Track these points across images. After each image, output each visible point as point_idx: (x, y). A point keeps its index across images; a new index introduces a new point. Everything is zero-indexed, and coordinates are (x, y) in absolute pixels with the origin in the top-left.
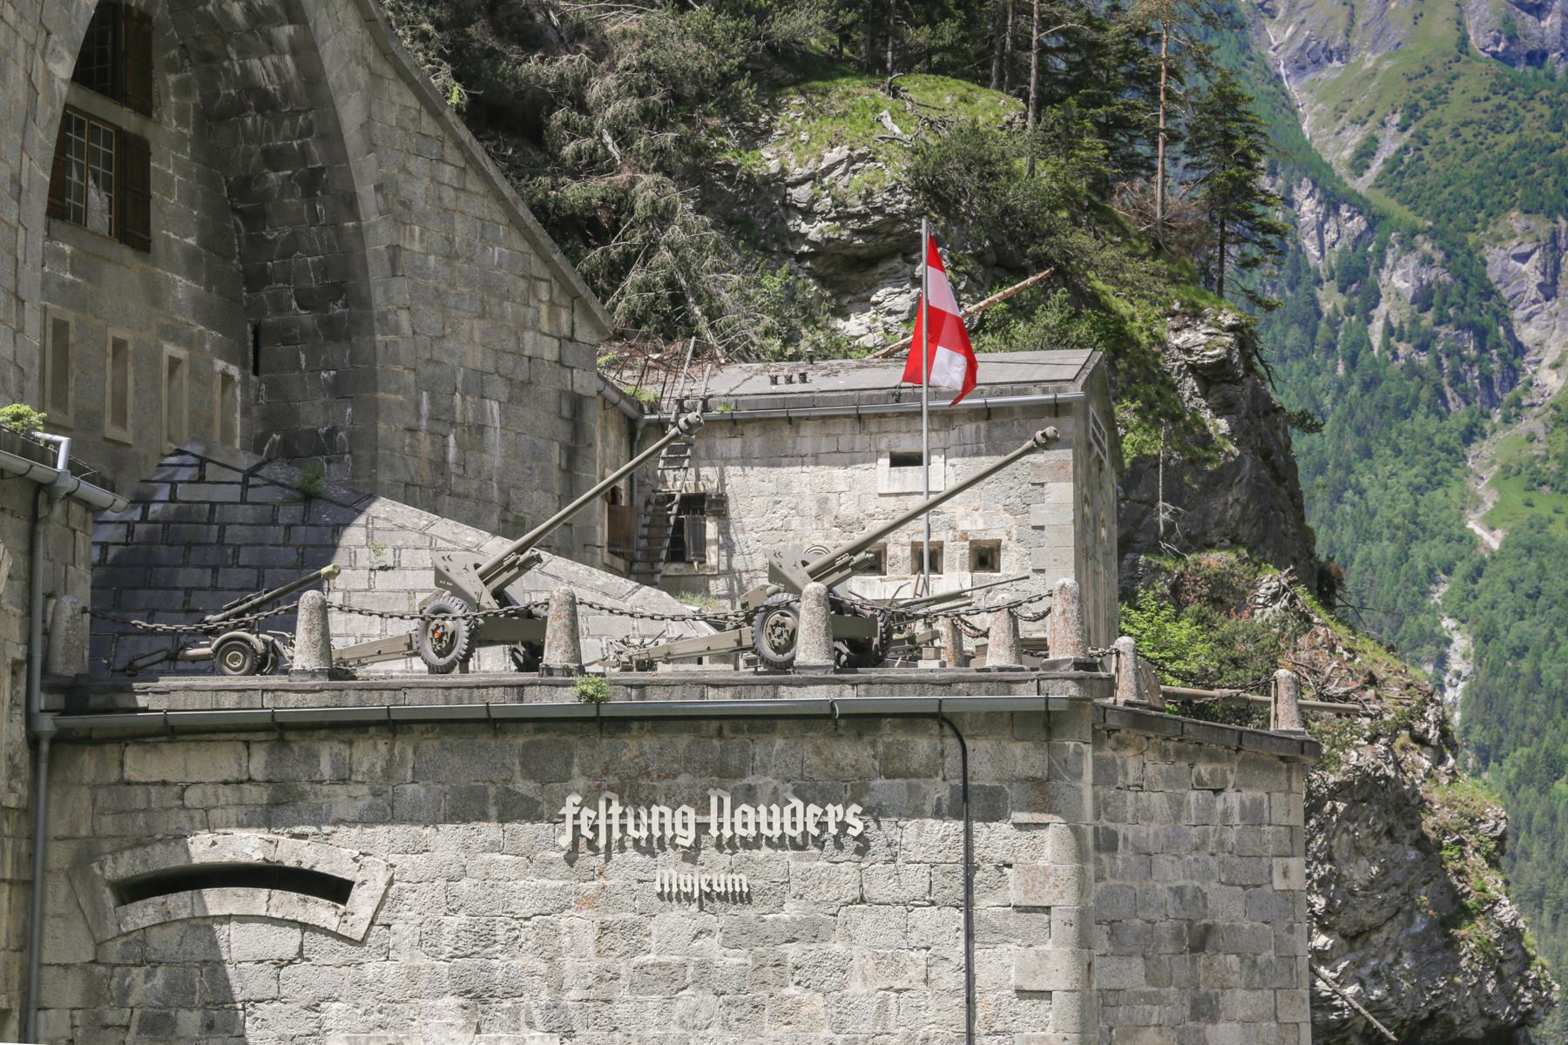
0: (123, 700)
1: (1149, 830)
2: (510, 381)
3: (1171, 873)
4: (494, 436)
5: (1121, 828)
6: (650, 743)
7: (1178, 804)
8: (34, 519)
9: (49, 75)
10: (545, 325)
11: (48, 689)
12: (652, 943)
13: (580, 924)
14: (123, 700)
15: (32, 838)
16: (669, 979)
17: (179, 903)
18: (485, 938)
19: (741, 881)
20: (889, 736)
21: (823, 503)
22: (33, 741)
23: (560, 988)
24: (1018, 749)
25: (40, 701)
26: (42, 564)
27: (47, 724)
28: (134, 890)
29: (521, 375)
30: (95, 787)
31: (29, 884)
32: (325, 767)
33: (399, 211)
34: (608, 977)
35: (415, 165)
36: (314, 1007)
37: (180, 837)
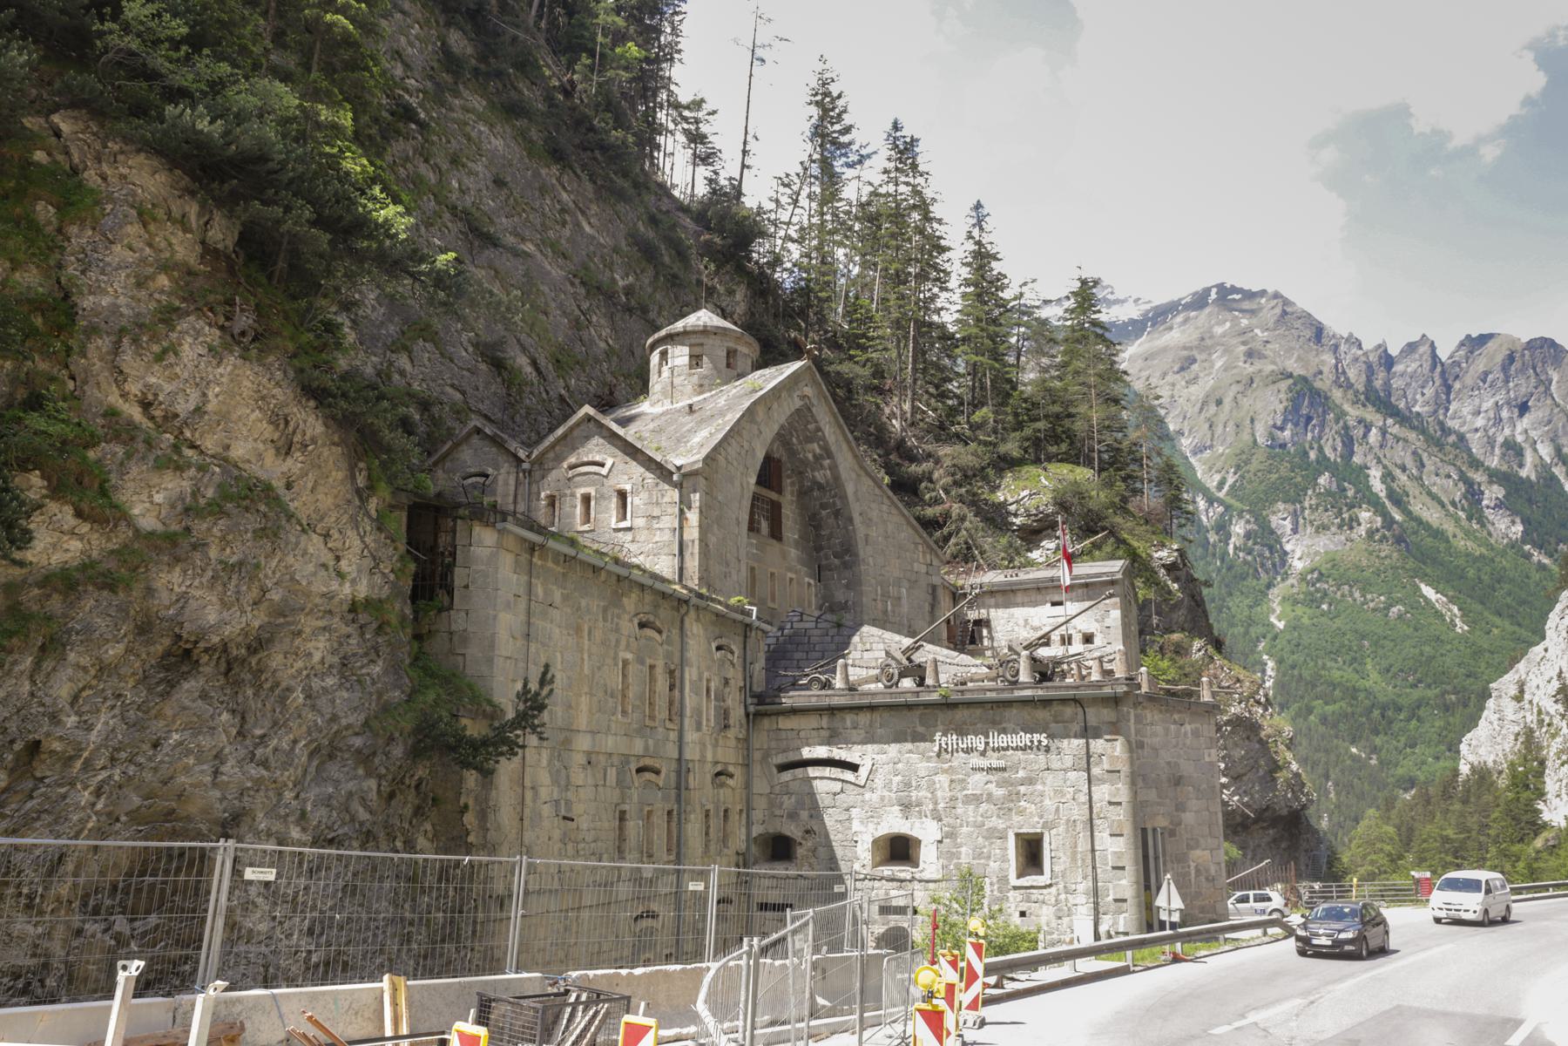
0: (777, 700)
1: (1156, 740)
4: (904, 601)
5: (1145, 740)
7: (1167, 730)
8: (746, 637)
9: (748, 483)
10: (921, 560)
11: (752, 697)
12: (970, 786)
13: (943, 780)
14: (777, 700)
15: (748, 749)
16: (976, 799)
17: (799, 772)
18: (908, 785)
19: (1002, 763)
20: (1056, 708)
21: (1026, 621)
22: (747, 715)
23: (936, 803)
24: (1105, 711)
25: (749, 701)
26: (748, 652)
27: (752, 709)
28: (784, 768)
29: (913, 579)
30: (768, 731)
31: (747, 765)
33: (868, 522)
34: (953, 799)
35: (873, 506)
36: (847, 810)
37: (799, 749)
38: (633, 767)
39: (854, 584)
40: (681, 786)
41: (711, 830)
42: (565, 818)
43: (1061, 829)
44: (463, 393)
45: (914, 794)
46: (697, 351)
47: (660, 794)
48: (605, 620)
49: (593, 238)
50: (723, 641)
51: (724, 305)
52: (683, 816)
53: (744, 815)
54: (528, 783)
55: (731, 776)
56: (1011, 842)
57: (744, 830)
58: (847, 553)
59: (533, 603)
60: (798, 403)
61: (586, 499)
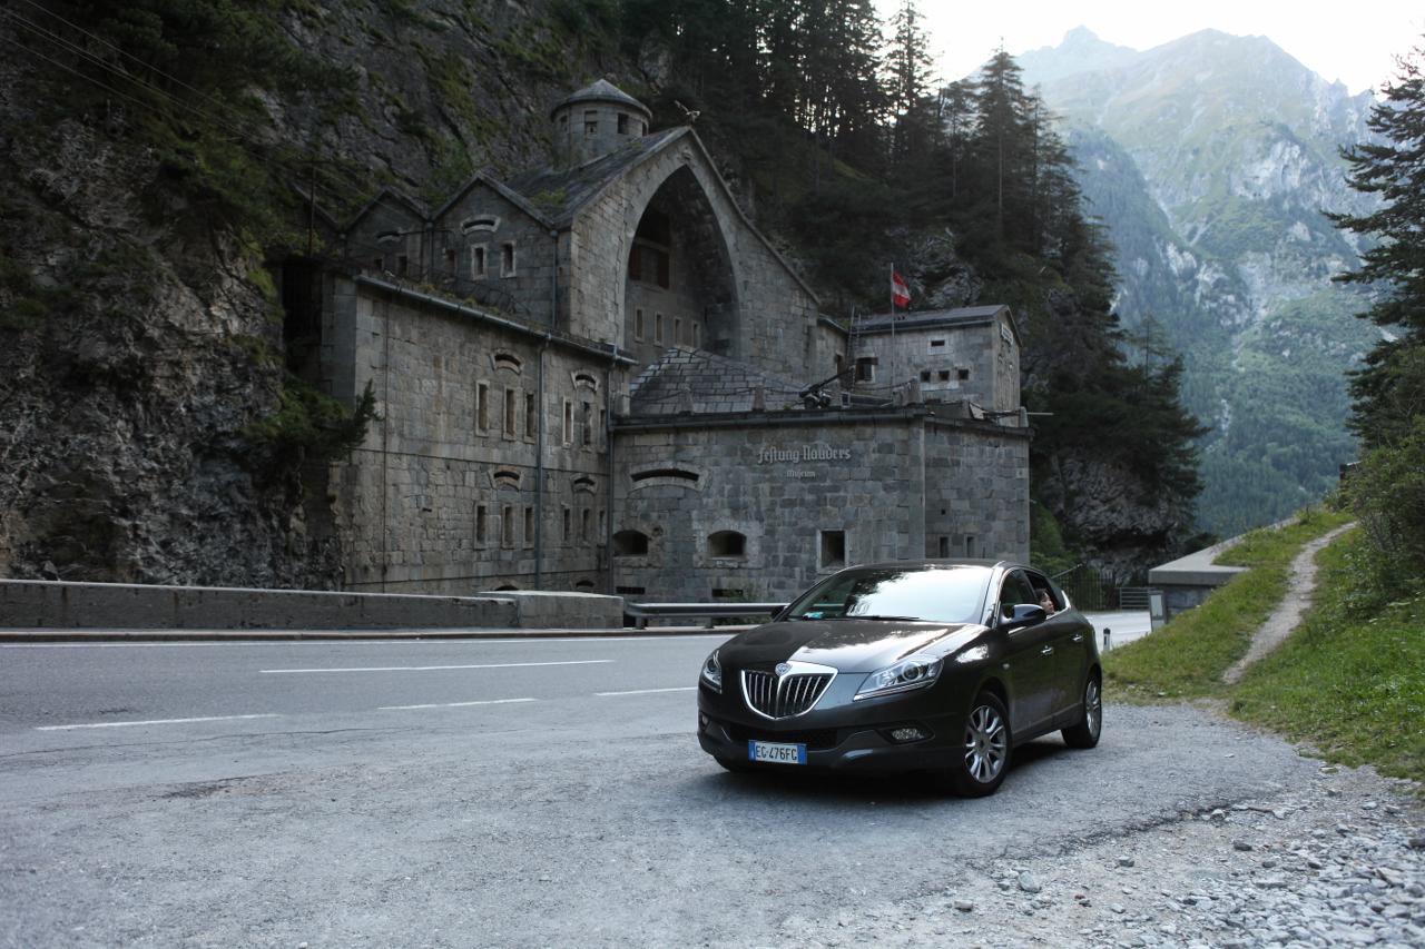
2: (786, 322)
3: (980, 473)
4: (781, 340)
6: (786, 432)
7: (982, 452)
13: (765, 487)
16: (790, 503)
18: (736, 492)
19: (813, 474)
20: (858, 429)
21: (909, 360)
22: (608, 433)
23: (759, 507)
24: (899, 431)
27: (611, 429)
28: (638, 477)
29: (790, 319)
31: (608, 476)
32: (690, 441)
33: (747, 269)
34: (773, 503)
38: (491, 471)
39: (732, 325)
40: (538, 489)
41: (571, 527)
42: (425, 510)
43: (859, 528)
44: (388, 160)
45: (741, 499)
46: (591, 118)
47: (518, 495)
48: (462, 354)
49: (515, 10)
50: (585, 372)
51: (647, 69)
52: (542, 514)
53: (605, 517)
54: (389, 482)
55: (592, 483)
56: (819, 538)
57: (604, 528)
58: (728, 298)
59: (390, 341)
60: (678, 165)
61: (480, 252)
